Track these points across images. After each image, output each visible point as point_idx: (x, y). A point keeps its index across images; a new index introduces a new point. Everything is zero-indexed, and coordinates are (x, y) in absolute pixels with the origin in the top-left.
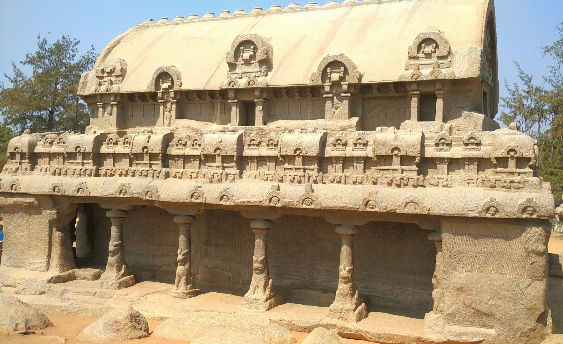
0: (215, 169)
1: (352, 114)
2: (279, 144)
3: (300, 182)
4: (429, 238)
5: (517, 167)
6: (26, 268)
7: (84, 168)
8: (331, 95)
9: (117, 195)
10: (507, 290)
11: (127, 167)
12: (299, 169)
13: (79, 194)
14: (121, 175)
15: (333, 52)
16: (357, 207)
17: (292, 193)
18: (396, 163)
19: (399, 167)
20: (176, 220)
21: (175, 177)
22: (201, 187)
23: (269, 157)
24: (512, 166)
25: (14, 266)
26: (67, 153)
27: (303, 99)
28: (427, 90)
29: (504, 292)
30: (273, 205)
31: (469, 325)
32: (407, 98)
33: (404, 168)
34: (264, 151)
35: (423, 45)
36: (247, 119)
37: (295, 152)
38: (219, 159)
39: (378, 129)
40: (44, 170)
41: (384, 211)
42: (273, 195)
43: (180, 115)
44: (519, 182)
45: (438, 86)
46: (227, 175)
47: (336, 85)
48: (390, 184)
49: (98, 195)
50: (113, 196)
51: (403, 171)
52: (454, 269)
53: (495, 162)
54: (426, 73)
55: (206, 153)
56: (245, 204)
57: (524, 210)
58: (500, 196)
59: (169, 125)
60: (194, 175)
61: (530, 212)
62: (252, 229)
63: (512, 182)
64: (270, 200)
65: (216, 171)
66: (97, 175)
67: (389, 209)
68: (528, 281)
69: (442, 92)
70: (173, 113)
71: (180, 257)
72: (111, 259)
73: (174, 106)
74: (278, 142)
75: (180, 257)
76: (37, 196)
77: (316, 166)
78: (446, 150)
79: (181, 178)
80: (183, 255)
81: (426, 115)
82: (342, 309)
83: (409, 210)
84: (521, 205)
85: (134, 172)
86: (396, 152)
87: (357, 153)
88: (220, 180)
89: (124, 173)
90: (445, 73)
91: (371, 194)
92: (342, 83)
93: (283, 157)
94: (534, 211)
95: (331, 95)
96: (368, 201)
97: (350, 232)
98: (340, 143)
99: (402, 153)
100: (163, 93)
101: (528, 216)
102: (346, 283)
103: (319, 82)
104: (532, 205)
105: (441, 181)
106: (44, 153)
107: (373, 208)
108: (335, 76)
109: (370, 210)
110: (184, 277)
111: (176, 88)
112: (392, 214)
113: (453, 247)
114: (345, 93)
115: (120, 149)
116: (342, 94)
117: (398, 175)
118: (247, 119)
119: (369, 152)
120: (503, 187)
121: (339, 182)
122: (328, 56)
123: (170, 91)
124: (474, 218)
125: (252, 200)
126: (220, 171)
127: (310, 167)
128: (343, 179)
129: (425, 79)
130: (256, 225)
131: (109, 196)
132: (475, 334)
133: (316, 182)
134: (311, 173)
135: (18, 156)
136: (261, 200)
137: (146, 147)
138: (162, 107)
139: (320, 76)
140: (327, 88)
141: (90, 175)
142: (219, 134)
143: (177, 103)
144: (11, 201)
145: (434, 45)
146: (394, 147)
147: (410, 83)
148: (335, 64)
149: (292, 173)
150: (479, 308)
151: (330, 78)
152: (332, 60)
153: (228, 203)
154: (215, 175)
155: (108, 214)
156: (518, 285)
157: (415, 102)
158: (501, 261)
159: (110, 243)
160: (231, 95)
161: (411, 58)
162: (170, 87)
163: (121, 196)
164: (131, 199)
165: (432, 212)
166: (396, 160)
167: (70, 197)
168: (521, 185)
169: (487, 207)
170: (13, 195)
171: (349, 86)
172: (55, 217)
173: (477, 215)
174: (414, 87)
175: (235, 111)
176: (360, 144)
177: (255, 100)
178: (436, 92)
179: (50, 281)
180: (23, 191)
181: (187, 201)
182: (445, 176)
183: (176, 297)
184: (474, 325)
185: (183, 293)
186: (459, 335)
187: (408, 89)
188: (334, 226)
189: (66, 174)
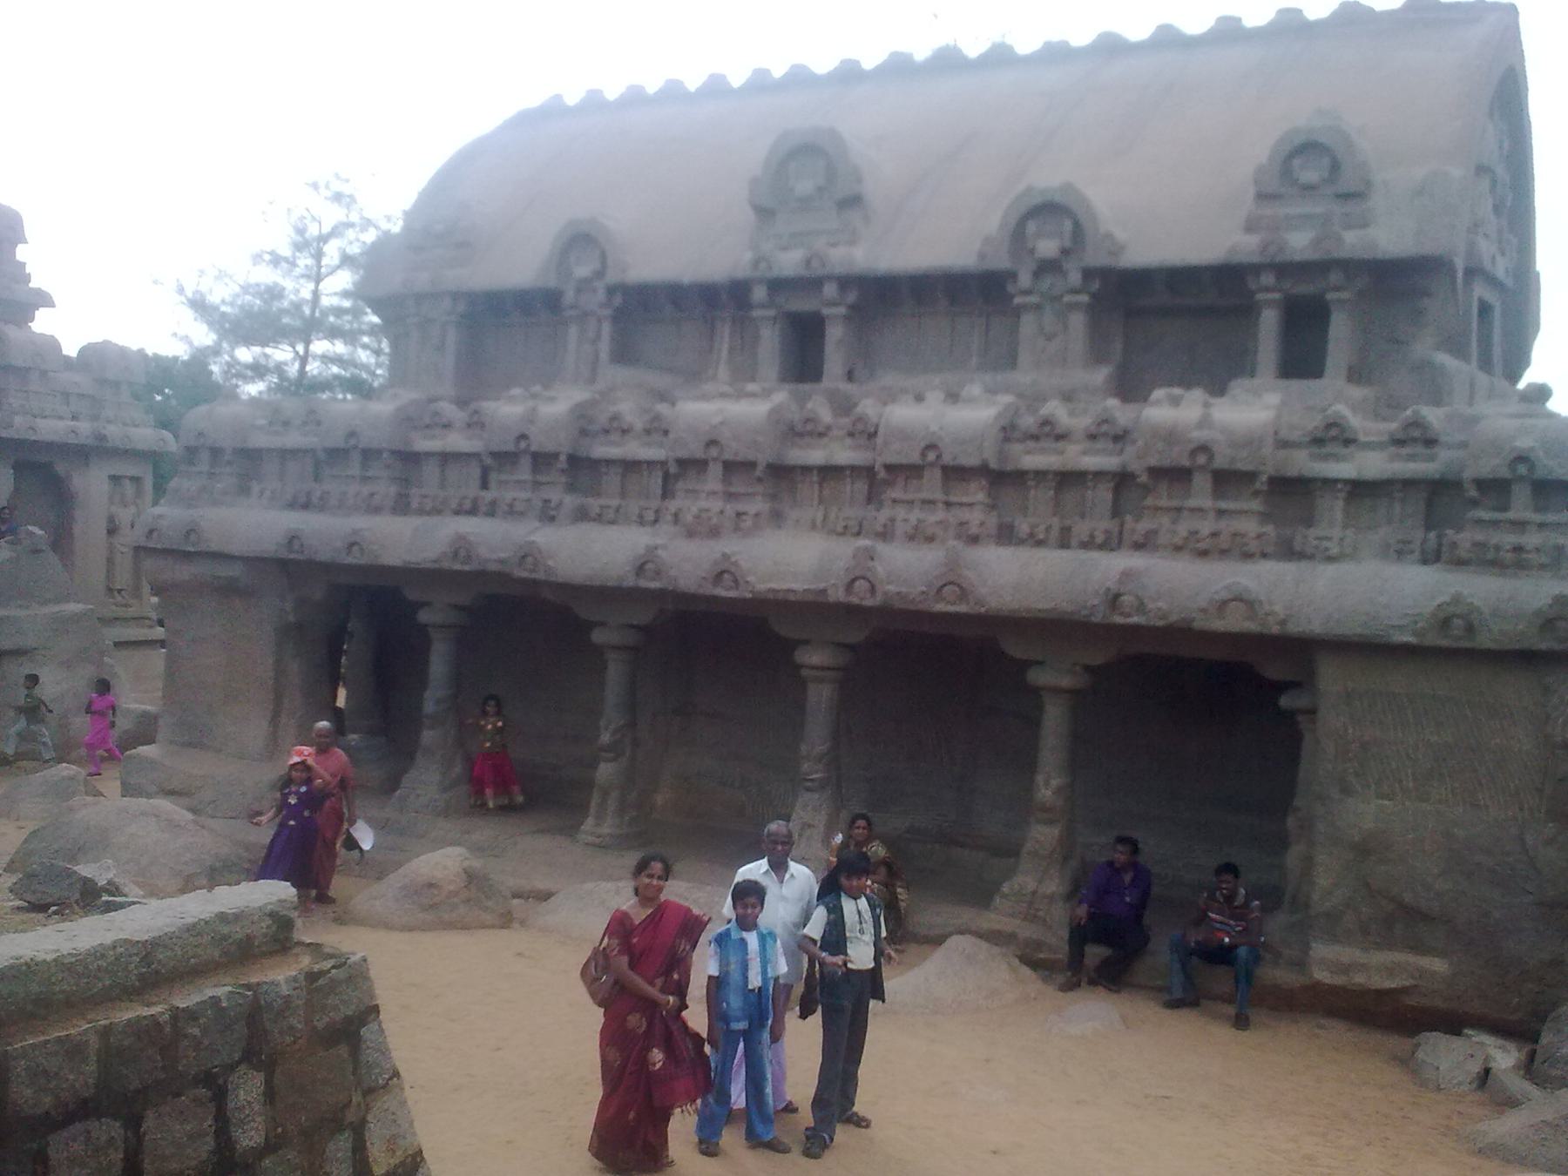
0: (704, 498)
1: (1097, 355)
2: (881, 431)
3: (930, 539)
4: (1285, 701)
5: (1537, 510)
7: (366, 490)
8: (1033, 299)
9: (446, 565)
11: (472, 490)
12: (931, 502)
14: (457, 513)
15: (1047, 178)
16: (1084, 612)
17: (907, 567)
18: (1201, 494)
19: (1208, 503)
20: (598, 636)
21: (598, 519)
22: (665, 547)
23: (853, 468)
24: (1522, 506)
25: (190, 745)
26: (326, 450)
28: (1304, 289)
30: (855, 600)
31: (1379, 947)
32: (1247, 311)
33: (1223, 505)
34: (844, 454)
35: (1296, 162)
37: (923, 455)
38: (715, 470)
39: (1159, 393)
40: (268, 493)
41: (1161, 623)
42: (858, 573)
43: (624, 354)
44: (1538, 550)
45: (1335, 277)
46: (739, 515)
47: (1048, 267)
51: (1221, 513)
52: (1346, 790)
53: (1473, 493)
54: (1299, 243)
55: (683, 453)
58: (1480, 589)
59: (592, 380)
60: (650, 516)
62: (802, 666)
63: (1518, 549)
64: (849, 586)
65: (703, 504)
66: (401, 506)
67: (1174, 618)
69: (1345, 295)
70: (605, 348)
71: (606, 738)
72: (428, 736)
73: (606, 328)
74: (877, 426)
75: (606, 738)
77: (981, 496)
78: (1343, 459)
79: (612, 522)
80: (615, 732)
81: (1301, 360)
82: (1034, 893)
83: (1235, 622)
85: (493, 503)
86: (1202, 459)
87: (1092, 462)
88: (715, 532)
89: (468, 505)
90: (1353, 243)
91: (1127, 575)
92: (1066, 266)
93: (889, 468)
95: (1033, 299)
97: (1066, 682)
98: (1050, 433)
99: (1220, 462)
100: (579, 291)
102: (1050, 822)
103: (1001, 262)
105: (1325, 544)
106: (269, 450)
107: (1129, 615)
108: (1047, 247)
109: (1118, 620)
110: (615, 794)
111: (612, 277)
112: (1181, 632)
115: (457, 442)
116: (1066, 299)
117: (1206, 527)
119: (1128, 458)
121: (1040, 543)
122: (1029, 190)
126: (716, 505)
127: (965, 500)
128: (1055, 533)
129: (1297, 258)
130: (813, 657)
132: (1391, 971)
133: (974, 540)
134: (965, 515)
135: (205, 456)
137: (523, 437)
138: (573, 331)
140: (1025, 280)
141: (377, 510)
143: (616, 319)
144: (184, 572)
145: (1326, 161)
147: (1256, 269)
148: (1048, 210)
149: (915, 515)
150: (1408, 898)
151: (1032, 251)
152: (1038, 200)
153: (732, 594)
154: (704, 515)
155: (424, 616)
157: (1269, 321)
159: (427, 694)
160: (759, 294)
161: (1263, 197)
162: (600, 274)
163: (457, 567)
164: (481, 575)
165: (1293, 628)
166: (1202, 482)
167: (328, 568)
168: (1544, 559)
170: (187, 556)
171: (1088, 274)
172: (291, 618)
174: (1268, 279)
175: (770, 340)
176: (1105, 434)
177: (826, 311)
178: (1330, 296)
180: (214, 547)
181: (625, 584)
182: (1336, 533)
183: (594, 845)
184: (1391, 946)
185: (611, 836)
186: (1346, 969)
187: (1253, 287)
188: (1026, 665)
189: (322, 507)
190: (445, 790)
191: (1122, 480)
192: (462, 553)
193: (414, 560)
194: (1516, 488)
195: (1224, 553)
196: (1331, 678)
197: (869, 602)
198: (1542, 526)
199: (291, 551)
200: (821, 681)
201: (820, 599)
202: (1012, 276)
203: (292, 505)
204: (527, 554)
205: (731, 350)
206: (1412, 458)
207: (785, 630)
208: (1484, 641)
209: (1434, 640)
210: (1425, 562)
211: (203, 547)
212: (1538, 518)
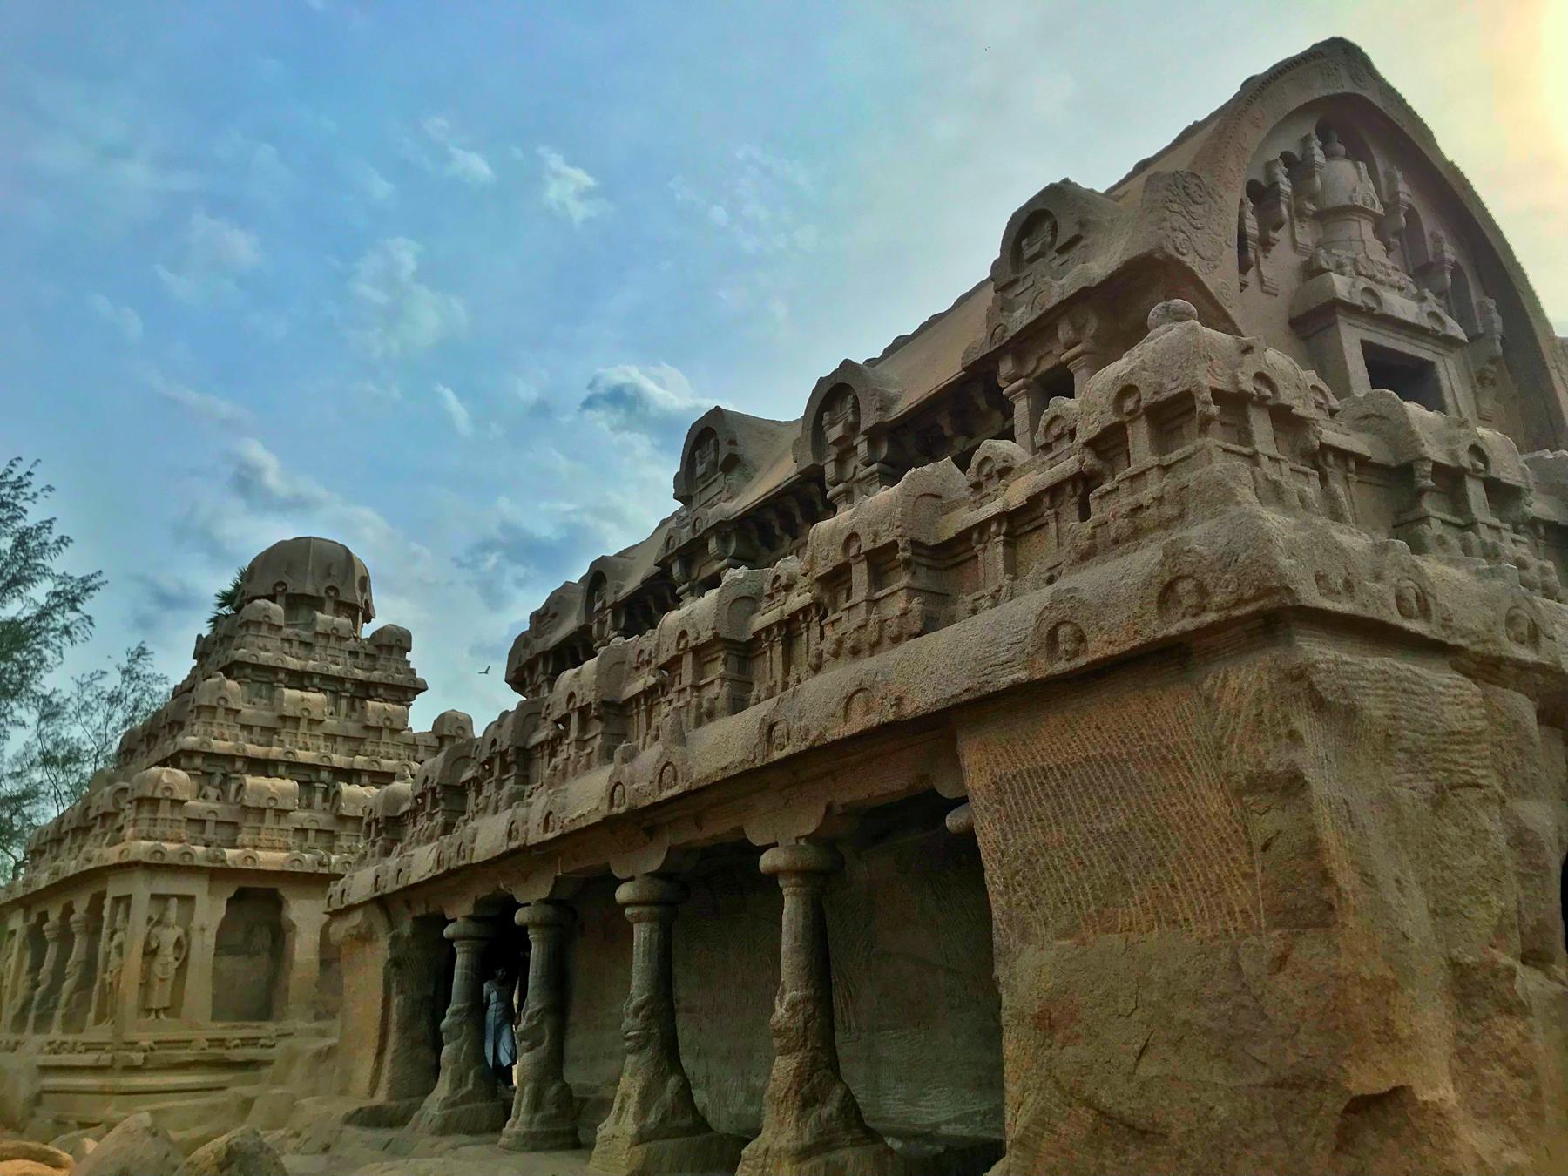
8: (841, 487)
10: (1197, 1000)
29: (1184, 1014)
35: (1024, 242)
45: (1064, 332)
52: (1024, 936)
57: (1167, 594)
61: (1188, 601)
63: (1137, 509)
68: (1273, 942)
84: (1147, 584)
94: (1202, 590)
96: (772, 726)
101: (1189, 624)
104: (1187, 570)
113: (1005, 839)
114: (868, 465)
120: (1116, 542)
139: (809, 444)
146: (846, 534)
150: (1105, 1098)
156: (1236, 967)
158: (1162, 864)
168: (1170, 510)
169: (1045, 629)
173: (1023, 675)
179: (349, 1120)
190: (447, 1107)
195: (875, 646)
196: (979, 766)
198: (1165, 469)
200: (639, 921)
208: (1098, 648)
209: (1047, 668)
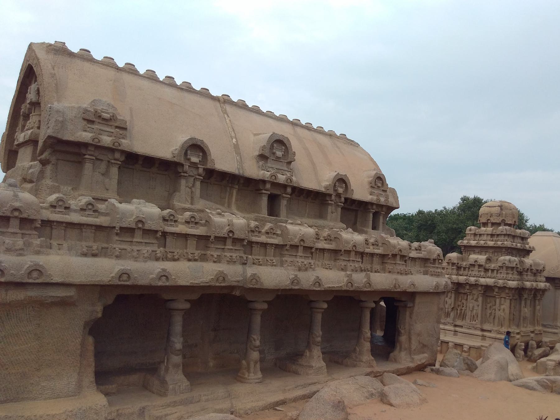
6: (35, 399)
9: (213, 284)
13: (160, 284)
27: (313, 200)
36: (273, 211)
48: (398, 273)
49: (188, 284)
50: (208, 284)
52: (416, 323)
56: (330, 289)
76: (81, 287)
118: (273, 211)
123: (199, 166)
124: (432, 293)
125: (335, 286)
131: (201, 285)
136: (341, 285)
142: (232, 218)
175: (264, 202)
191: (383, 256)
192: (221, 278)
193: (196, 282)
194: (228, 240)
196: (418, 300)
197: (351, 289)
199: (120, 281)
201: (340, 289)
202: (330, 195)
203: (85, 255)
204: (164, 275)
205: (236, 200)
206: (419, 253)
207: (166, 296)
210: (424, 275)
211: (48, 280)
212: (234, 248)
